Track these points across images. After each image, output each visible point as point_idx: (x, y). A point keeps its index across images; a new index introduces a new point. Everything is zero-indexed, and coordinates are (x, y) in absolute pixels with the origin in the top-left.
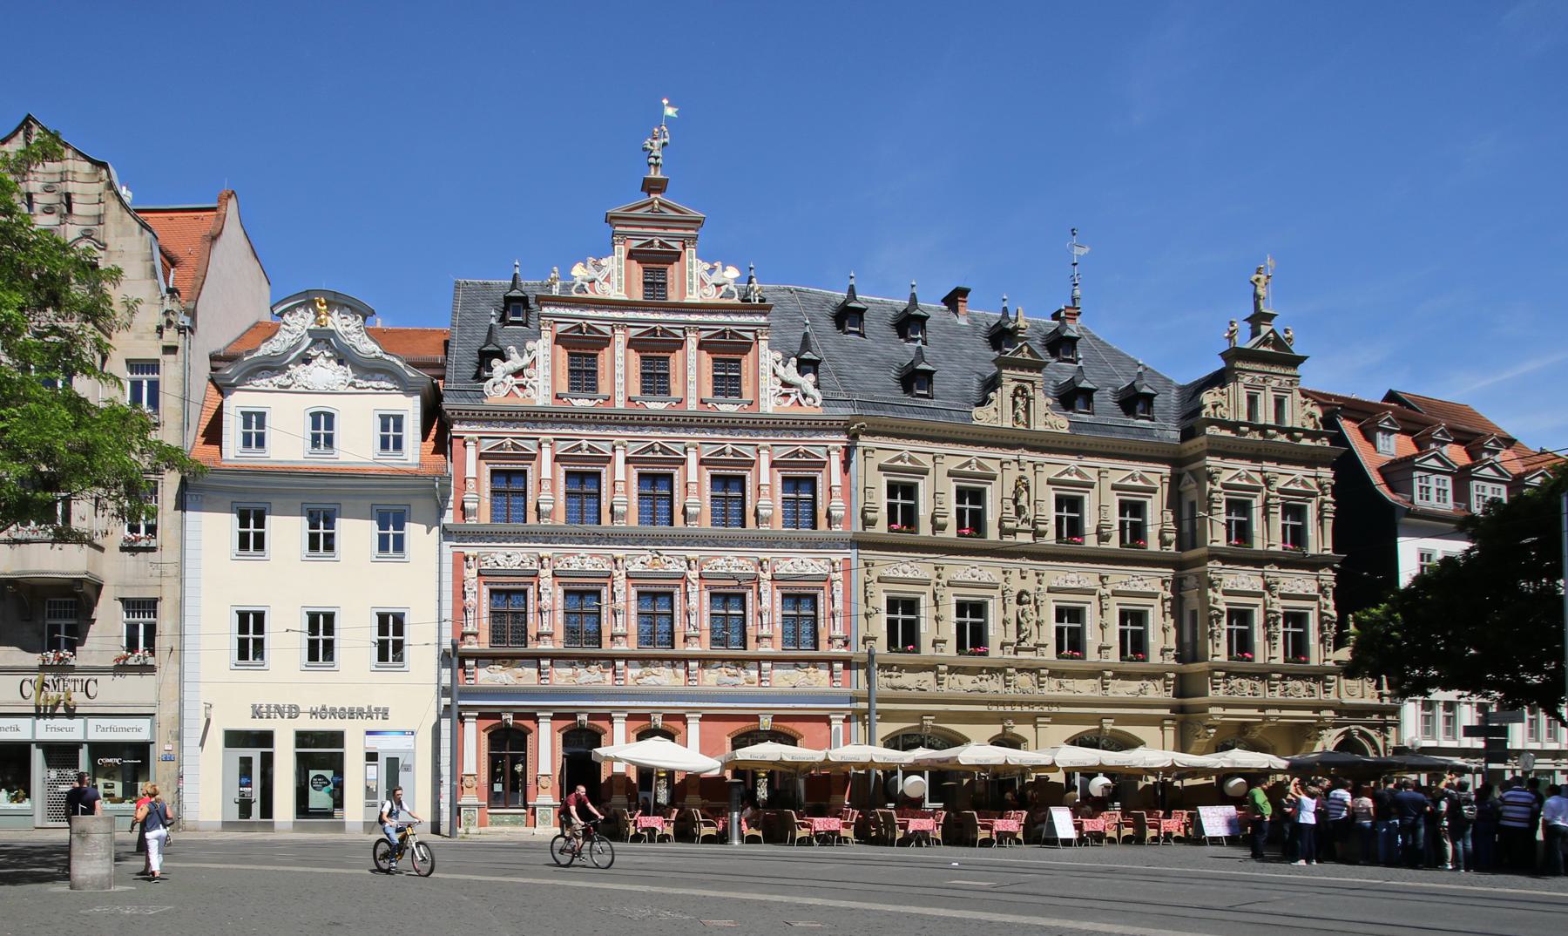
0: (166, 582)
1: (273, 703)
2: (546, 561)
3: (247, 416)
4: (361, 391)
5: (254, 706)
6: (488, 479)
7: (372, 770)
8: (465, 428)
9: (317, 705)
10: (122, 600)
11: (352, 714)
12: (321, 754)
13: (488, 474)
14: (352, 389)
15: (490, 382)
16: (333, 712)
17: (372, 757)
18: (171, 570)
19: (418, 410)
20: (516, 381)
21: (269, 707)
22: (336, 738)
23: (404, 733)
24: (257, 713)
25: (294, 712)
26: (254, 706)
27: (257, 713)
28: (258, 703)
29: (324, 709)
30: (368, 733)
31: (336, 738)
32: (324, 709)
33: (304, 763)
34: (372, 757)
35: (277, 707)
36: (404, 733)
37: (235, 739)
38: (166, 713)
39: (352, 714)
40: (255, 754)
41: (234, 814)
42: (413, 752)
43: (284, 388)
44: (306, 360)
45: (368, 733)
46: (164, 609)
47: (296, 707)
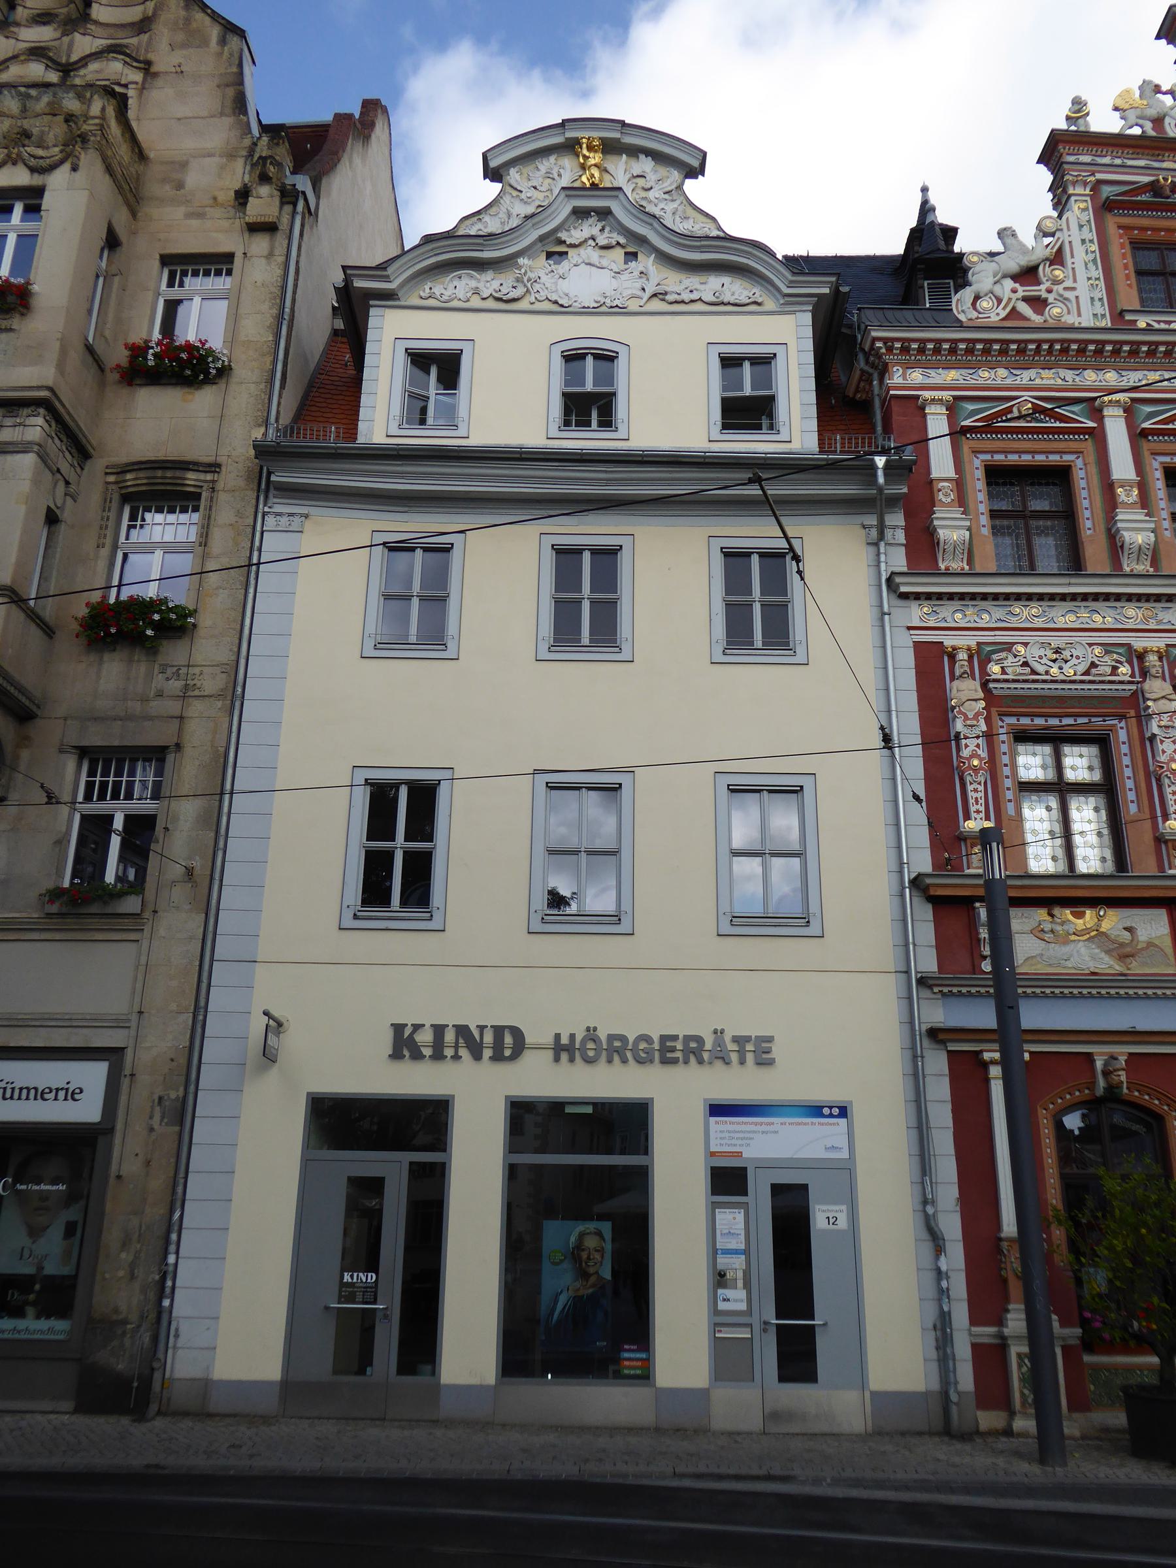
0: (196, 709)
1: (451, 1019)
2: (1152, 659)
3: (420, 360)
4: (679, 306)
5: (398, 1029)
6: (981, 485)
7: (731, 1220)
8: (916, 376)
9: (572, 1027)
10: (83, 752)
11: (670, 1051)
12: (583, 1163)
13: (980, 474)
14: (656, 305)
15: (967, 294)
16: (617, 1049)
17: (728, 1181)
18: (211, 683)
19: (809, 345)
20: (1022, 291)
21: (439, 1030)
22: (626, 1124)
23: (816, 1110)
24: (404, 1044)
25: (507, 1044)
26: (398, 1029)
27: (404, 1044)
28: (410, 1020)
29: (591, 1034)
30: (718, 1110)
31: (626, 1124)
32: (591, 1034)
33: (532, 1203)
34: (728, 1181)
35: (462, 1031)
36: (816, 1110)
37: (339, 1121)
38: (157, 1044)
39: (670, 1051)
40: (392, 1167)
41: (320, 1364)
42: (847, 1169)
43: (506, 303)
44: (555, 250)
45: (718, 1110)
46: (188, 771)
47: (517, 1033)
